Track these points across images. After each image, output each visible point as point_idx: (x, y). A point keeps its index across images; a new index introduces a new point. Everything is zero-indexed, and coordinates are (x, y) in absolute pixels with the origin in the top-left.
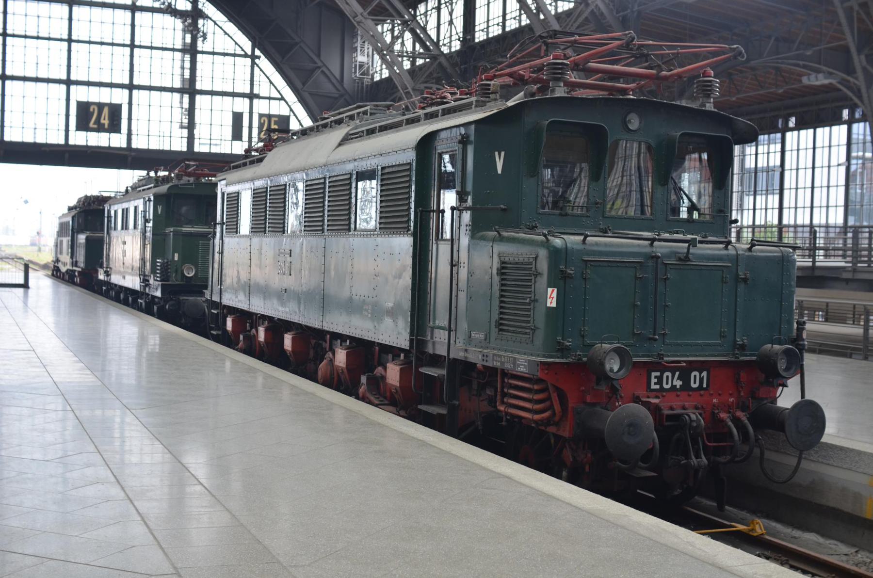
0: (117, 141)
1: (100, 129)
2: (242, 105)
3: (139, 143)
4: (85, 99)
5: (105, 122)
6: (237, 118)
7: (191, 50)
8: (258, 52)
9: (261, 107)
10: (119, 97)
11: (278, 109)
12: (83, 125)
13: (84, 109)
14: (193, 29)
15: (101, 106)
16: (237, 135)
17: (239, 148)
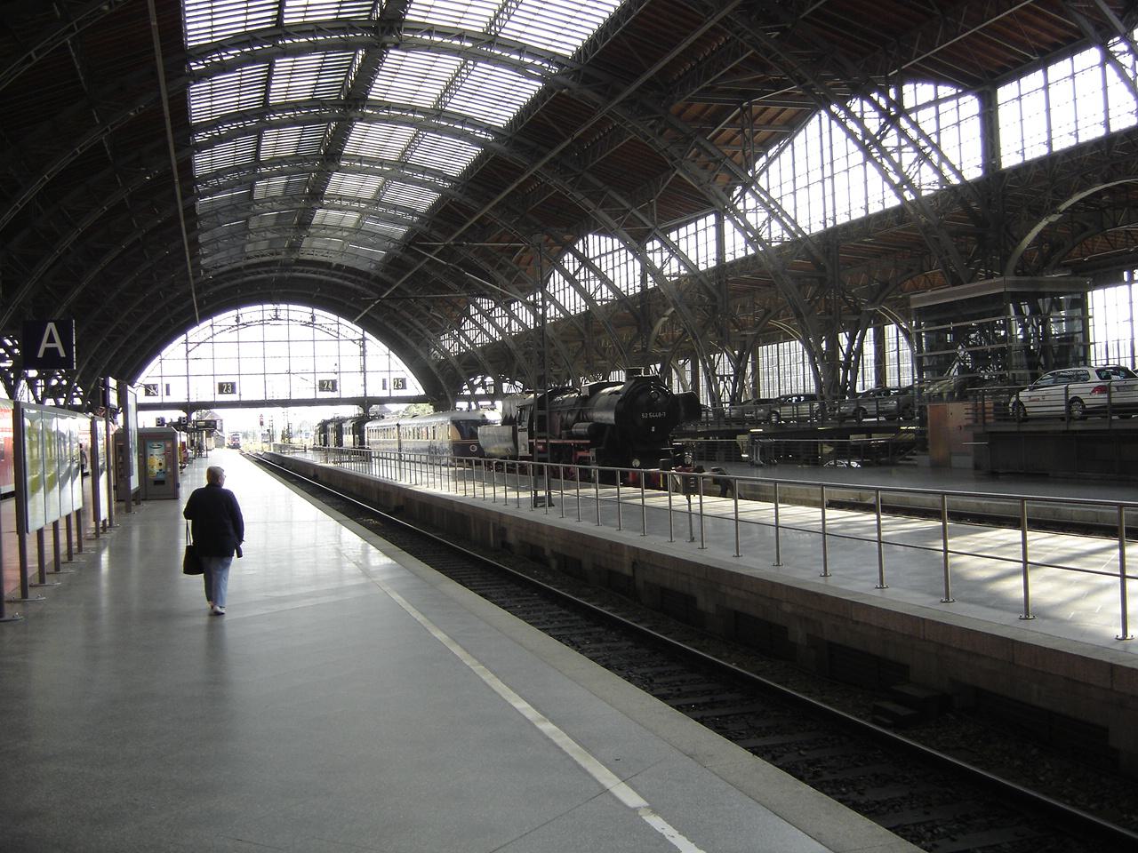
0: (334, 395)
1: (328, 390)
2: (386, 376)
4: (321, 379)
5: (331, 387)
6: (384, 381)
7: (363, 354)
8: (391, 352)
9: (395, 375)
10: (333, 377)
11: (401, 375)
12: (322, 389)
13: (322, 383)
14: (363, 346)
15: (328, 381)
16: (384, 388)
17: (385, 394)
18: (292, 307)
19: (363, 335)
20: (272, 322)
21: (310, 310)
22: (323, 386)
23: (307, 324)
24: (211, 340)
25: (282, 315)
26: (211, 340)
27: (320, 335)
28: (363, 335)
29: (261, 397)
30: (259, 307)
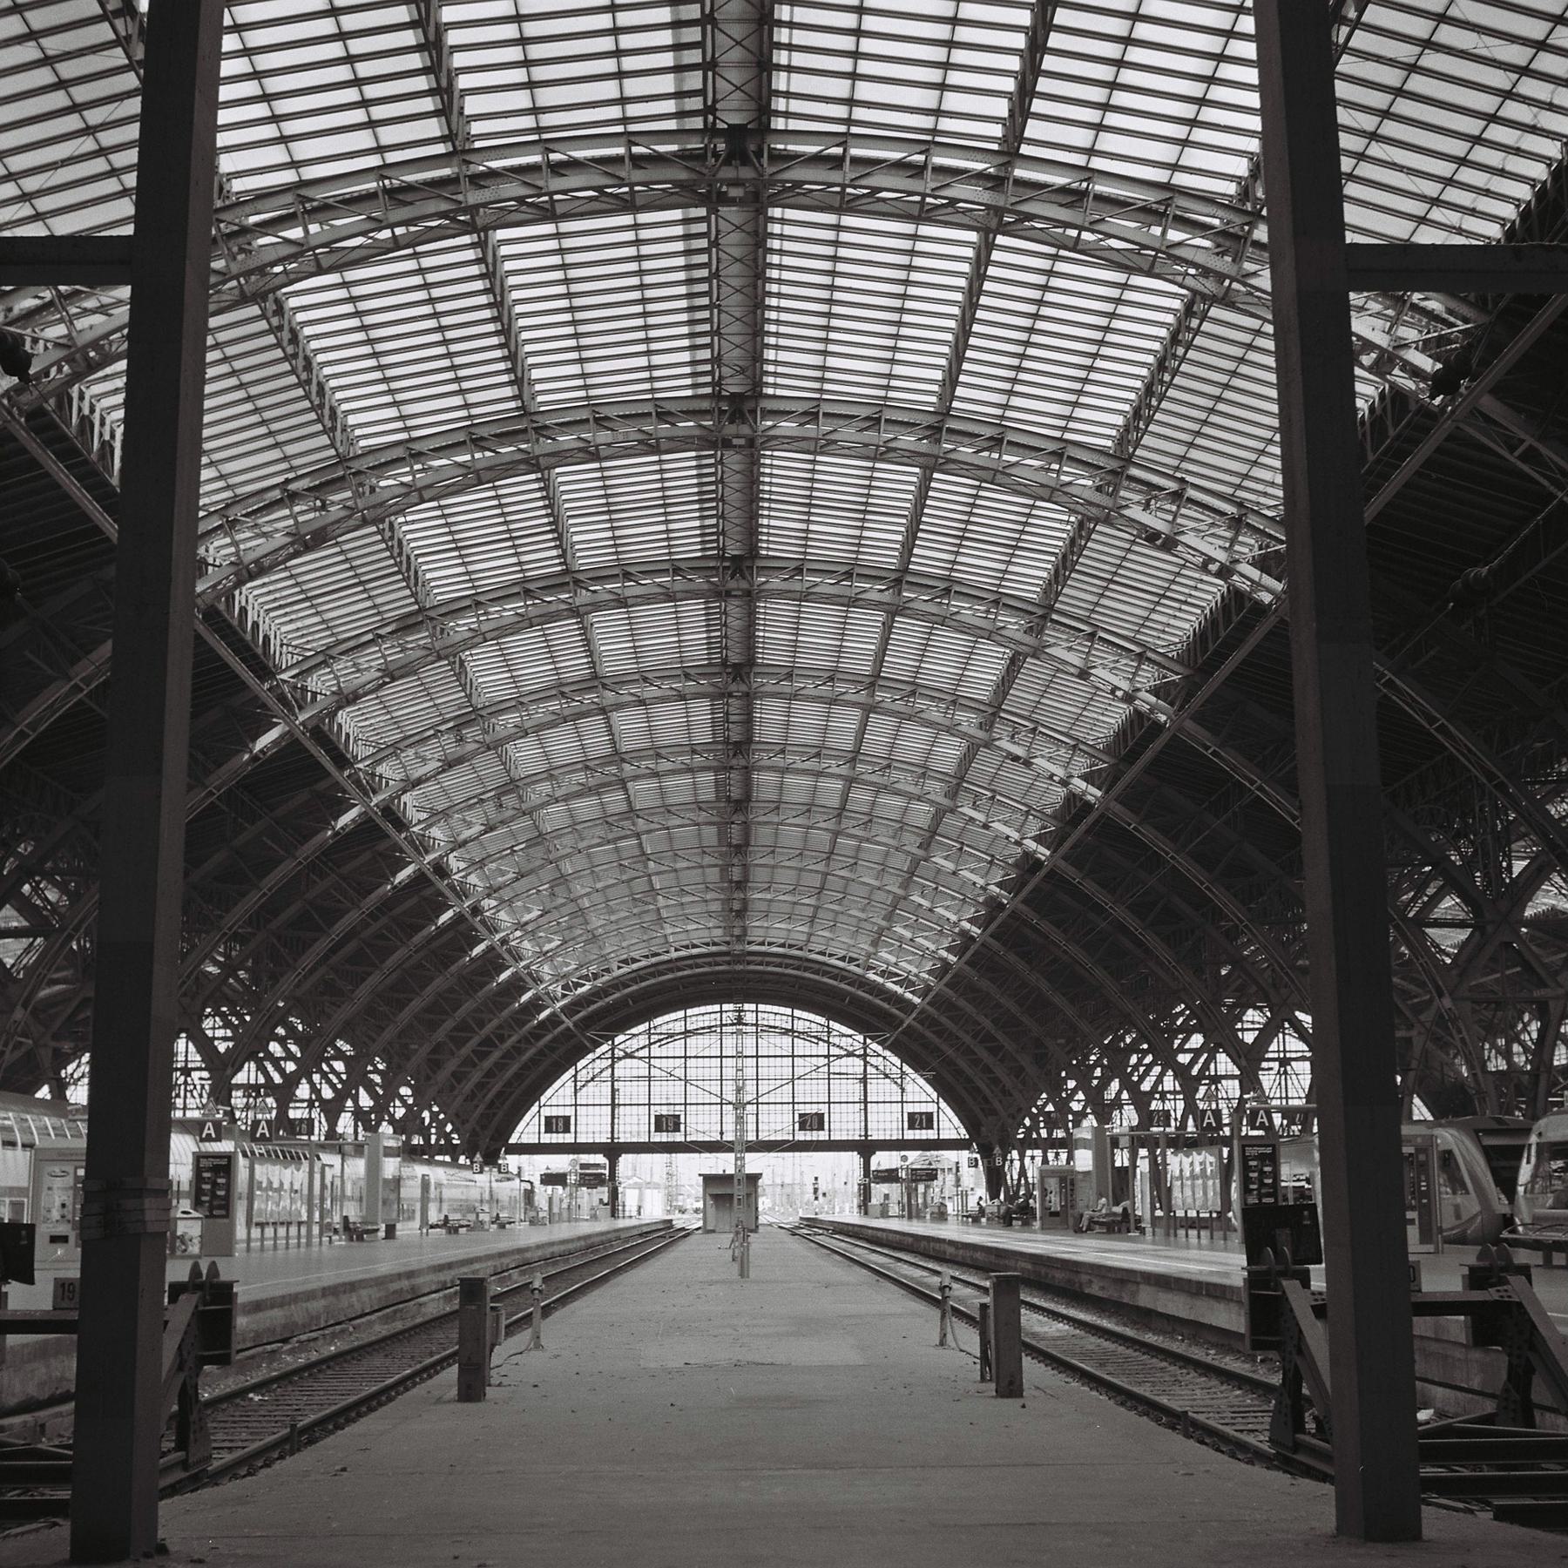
0: (822, 1136)
3: (836, 1136)
9: (909, 1108)
10: (824, 1109)
18: (761, 1007)
19: (865, 1046)
20: (734, 1029)
21: (788, 1011)
22: (807, 1122)
23: (786, 1032)
24: (644, 1053)
25: (749, 1018)
26: (644, 1053)
27: (802, 1047)
28: (865, 1046)
29: (716, 1137)
30: (717, 1007)
